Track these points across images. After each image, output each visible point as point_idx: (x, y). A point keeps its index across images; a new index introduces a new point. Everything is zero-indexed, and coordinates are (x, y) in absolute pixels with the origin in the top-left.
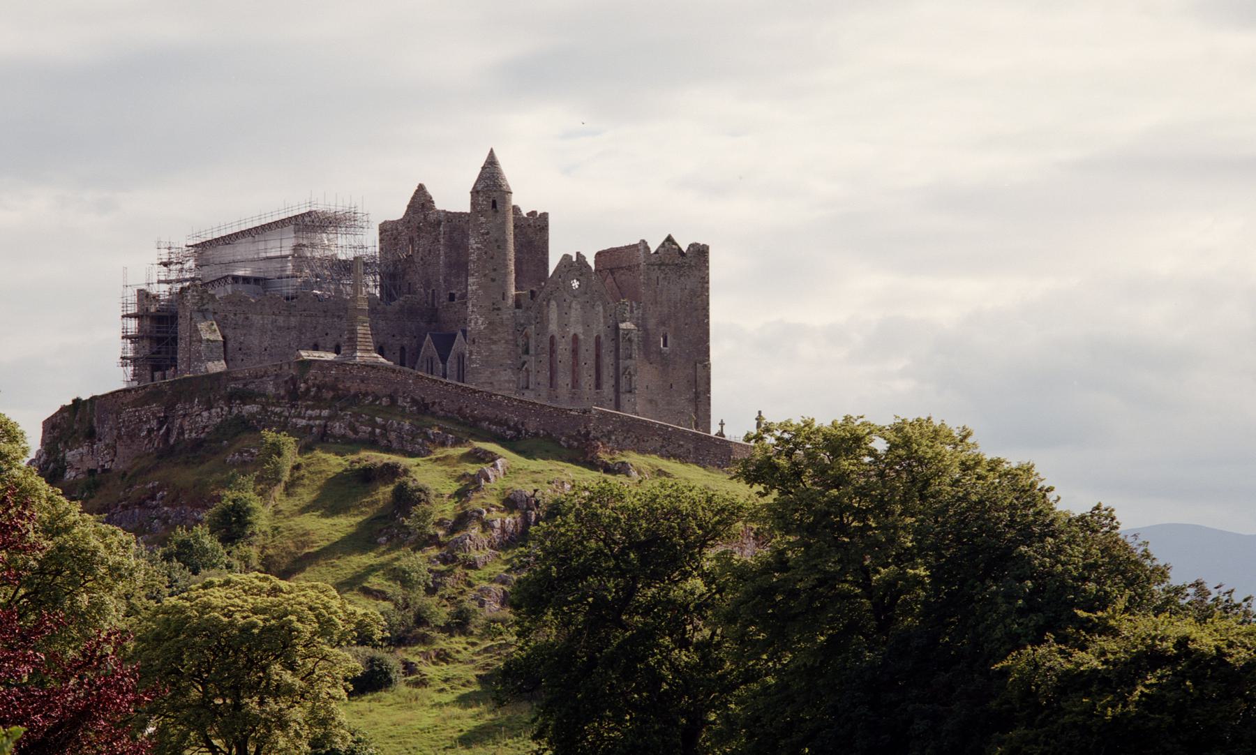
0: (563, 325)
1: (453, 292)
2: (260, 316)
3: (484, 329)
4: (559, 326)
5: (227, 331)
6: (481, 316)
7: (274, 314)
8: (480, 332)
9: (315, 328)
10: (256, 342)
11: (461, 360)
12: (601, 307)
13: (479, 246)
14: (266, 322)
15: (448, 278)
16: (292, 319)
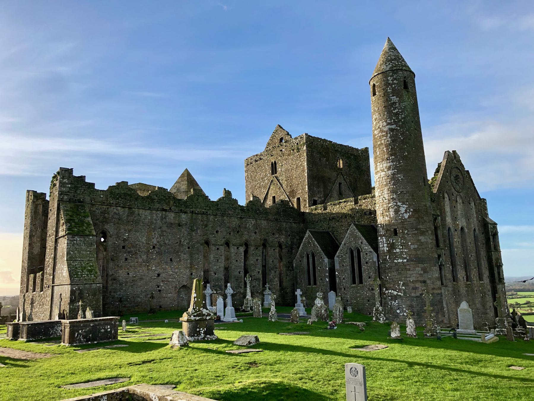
0: (455, 219)
1: (316, 199)
2: (149, 211)
3: (409, 217)
4: (452, 219)
5: (107, 227)
6: (404, 203)
7: (163, 210)
8: (403, 221)
9: (206, 226)
10: (144, 240)
11: (355, 254)
12: (473, 203)
13: (393, 127)
14: (155, 217)
15: (312, 187)
16: (183, 216)
